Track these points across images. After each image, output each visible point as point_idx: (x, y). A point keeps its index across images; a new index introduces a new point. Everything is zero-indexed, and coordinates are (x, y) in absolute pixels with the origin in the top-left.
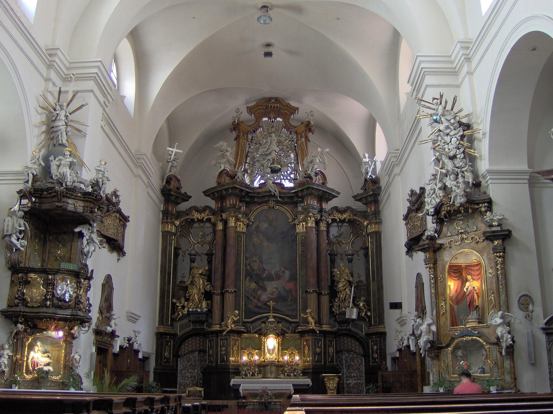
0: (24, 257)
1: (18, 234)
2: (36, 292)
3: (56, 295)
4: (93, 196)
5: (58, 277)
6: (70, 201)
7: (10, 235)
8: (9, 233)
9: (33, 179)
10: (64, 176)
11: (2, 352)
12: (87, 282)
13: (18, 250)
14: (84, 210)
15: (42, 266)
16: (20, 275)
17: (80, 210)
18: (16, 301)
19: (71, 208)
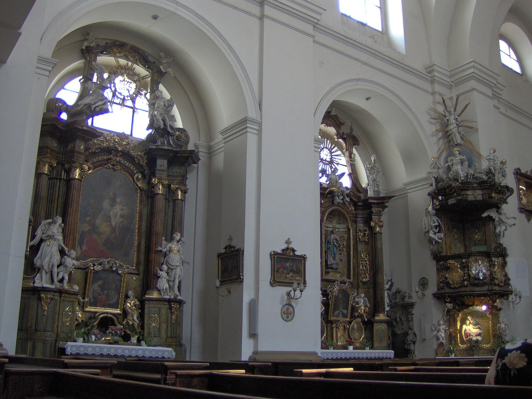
0: (444, 247)
1: (434, 229)
2: (456, 276)
3: (472, 276)
4: (487, 183)
5: (471, 259)
6: (469, 193)
7: (428, 232)
8: (427, 230)
9: (436, 182)
10: (457, 173)
11: (439, 327)
12: (500, 259)
13: (437, 242)
14: (483, 197)
15: (466, 251)
16: (441, 263)
17: (480, 198)
18: (442, 285)
19: (471, 198)
